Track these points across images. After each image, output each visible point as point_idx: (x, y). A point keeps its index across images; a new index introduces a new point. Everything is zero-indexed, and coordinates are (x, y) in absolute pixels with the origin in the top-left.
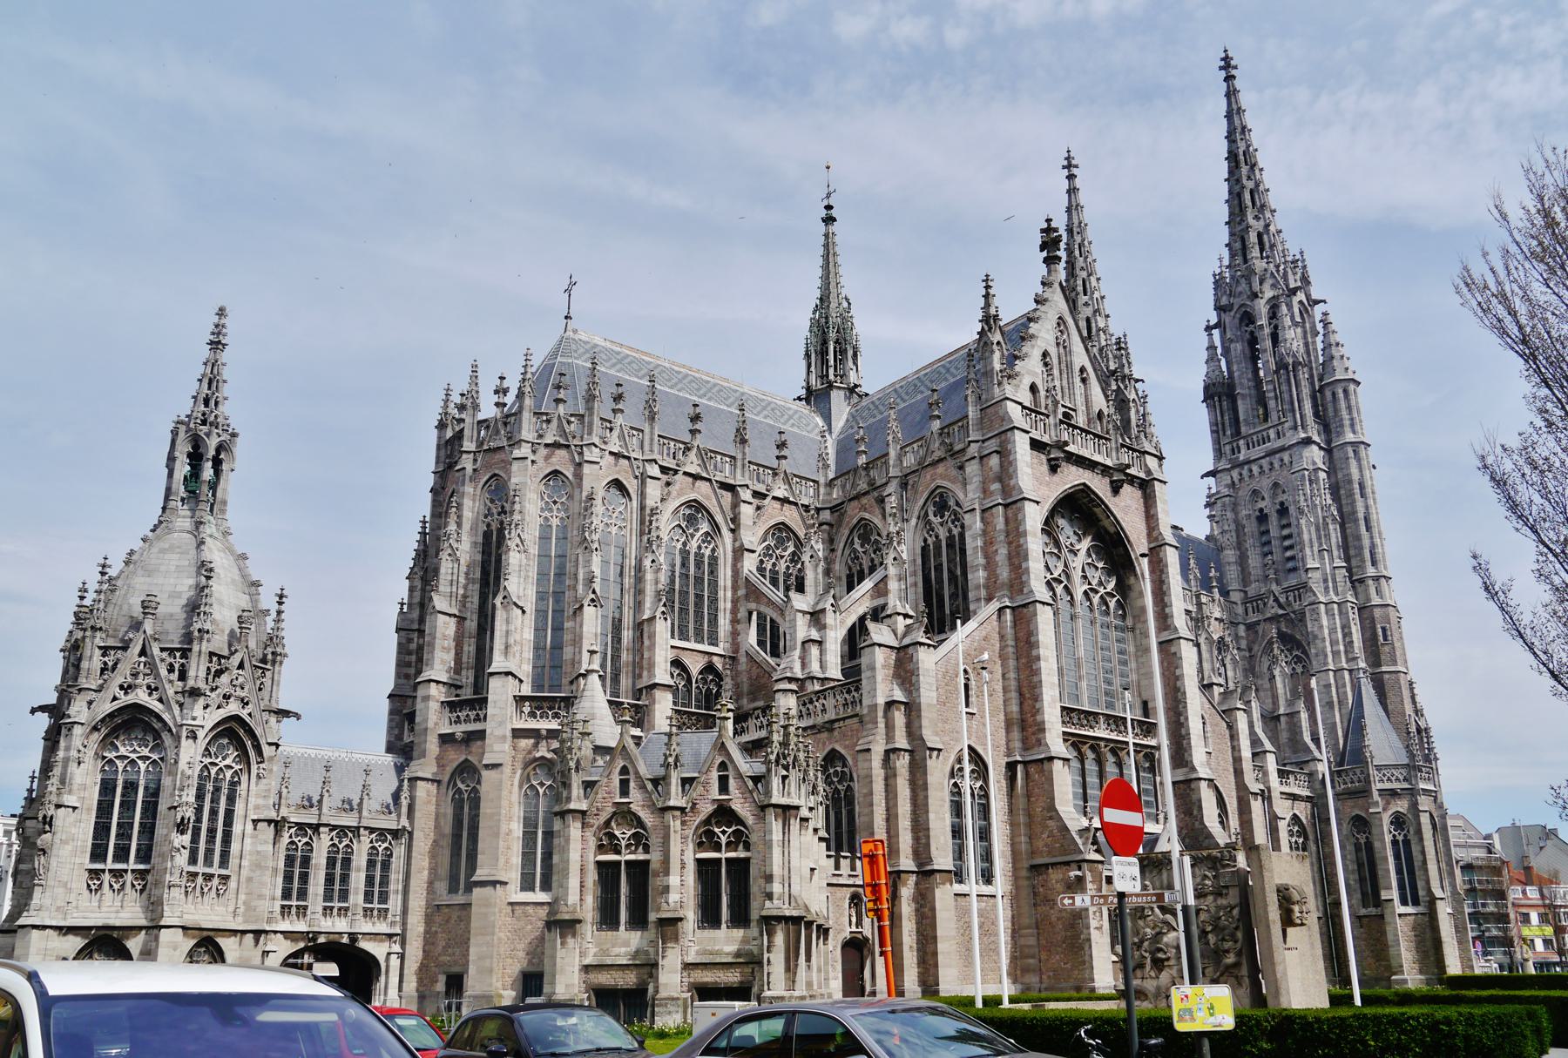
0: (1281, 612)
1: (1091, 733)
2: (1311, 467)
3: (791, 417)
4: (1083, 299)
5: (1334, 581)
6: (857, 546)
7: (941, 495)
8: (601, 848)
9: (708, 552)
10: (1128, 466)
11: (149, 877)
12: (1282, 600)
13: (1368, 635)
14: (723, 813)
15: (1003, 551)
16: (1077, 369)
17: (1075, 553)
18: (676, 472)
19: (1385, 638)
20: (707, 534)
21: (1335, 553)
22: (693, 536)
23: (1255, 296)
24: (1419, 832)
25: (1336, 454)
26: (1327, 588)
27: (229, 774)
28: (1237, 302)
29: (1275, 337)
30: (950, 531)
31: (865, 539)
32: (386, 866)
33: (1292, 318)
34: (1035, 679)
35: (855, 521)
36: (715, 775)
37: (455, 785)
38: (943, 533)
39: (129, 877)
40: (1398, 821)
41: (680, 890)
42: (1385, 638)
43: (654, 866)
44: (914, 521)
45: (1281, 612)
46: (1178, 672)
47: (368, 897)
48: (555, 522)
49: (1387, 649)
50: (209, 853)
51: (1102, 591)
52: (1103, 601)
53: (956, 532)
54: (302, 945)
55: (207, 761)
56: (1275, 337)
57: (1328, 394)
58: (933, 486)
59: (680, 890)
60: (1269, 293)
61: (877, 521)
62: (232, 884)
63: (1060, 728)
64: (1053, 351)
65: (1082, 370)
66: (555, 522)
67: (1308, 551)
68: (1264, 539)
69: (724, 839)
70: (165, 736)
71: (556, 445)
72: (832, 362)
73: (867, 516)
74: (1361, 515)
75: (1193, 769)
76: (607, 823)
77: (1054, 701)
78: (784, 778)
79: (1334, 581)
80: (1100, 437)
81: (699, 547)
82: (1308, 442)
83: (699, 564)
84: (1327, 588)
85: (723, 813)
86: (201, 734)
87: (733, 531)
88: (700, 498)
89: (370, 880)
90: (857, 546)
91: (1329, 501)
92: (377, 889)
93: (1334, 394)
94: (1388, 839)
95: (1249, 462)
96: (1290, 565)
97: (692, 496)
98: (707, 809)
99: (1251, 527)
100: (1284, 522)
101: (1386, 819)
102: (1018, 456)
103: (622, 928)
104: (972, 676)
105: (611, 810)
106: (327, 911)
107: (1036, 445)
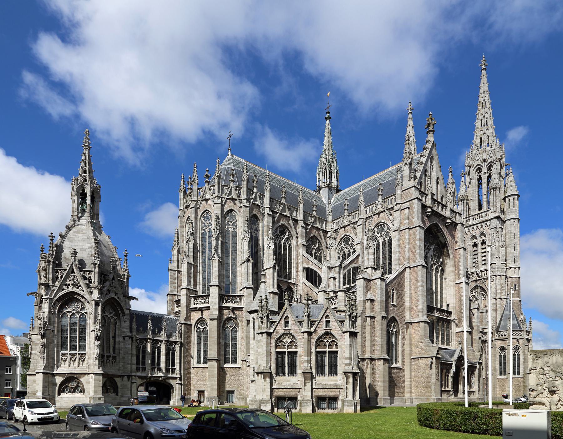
6: (343, 245)
7: (381, 225)
8: (277, 346)
9: (288, 245)
12: (480, 274)
14: (328, 334)
18: (277, 213)
20: (287, 238)
30: (384, 239)
31: (347, 242)
35: (342, 236)
36: (324, 320)
38: (381, 240)
43: (298, 353)
52: (437, 268)
53: (387, 239)
58: (378, 222)
61: (353, 235)
69: (327, 344)
72: (328, 177)
73: (348, 234)
76: (280, 337)
83: (285, 249)
85: (328, 334)
90: (343, 245)
96: (484, 262)
98: (321, 332)
105: (283, 332)
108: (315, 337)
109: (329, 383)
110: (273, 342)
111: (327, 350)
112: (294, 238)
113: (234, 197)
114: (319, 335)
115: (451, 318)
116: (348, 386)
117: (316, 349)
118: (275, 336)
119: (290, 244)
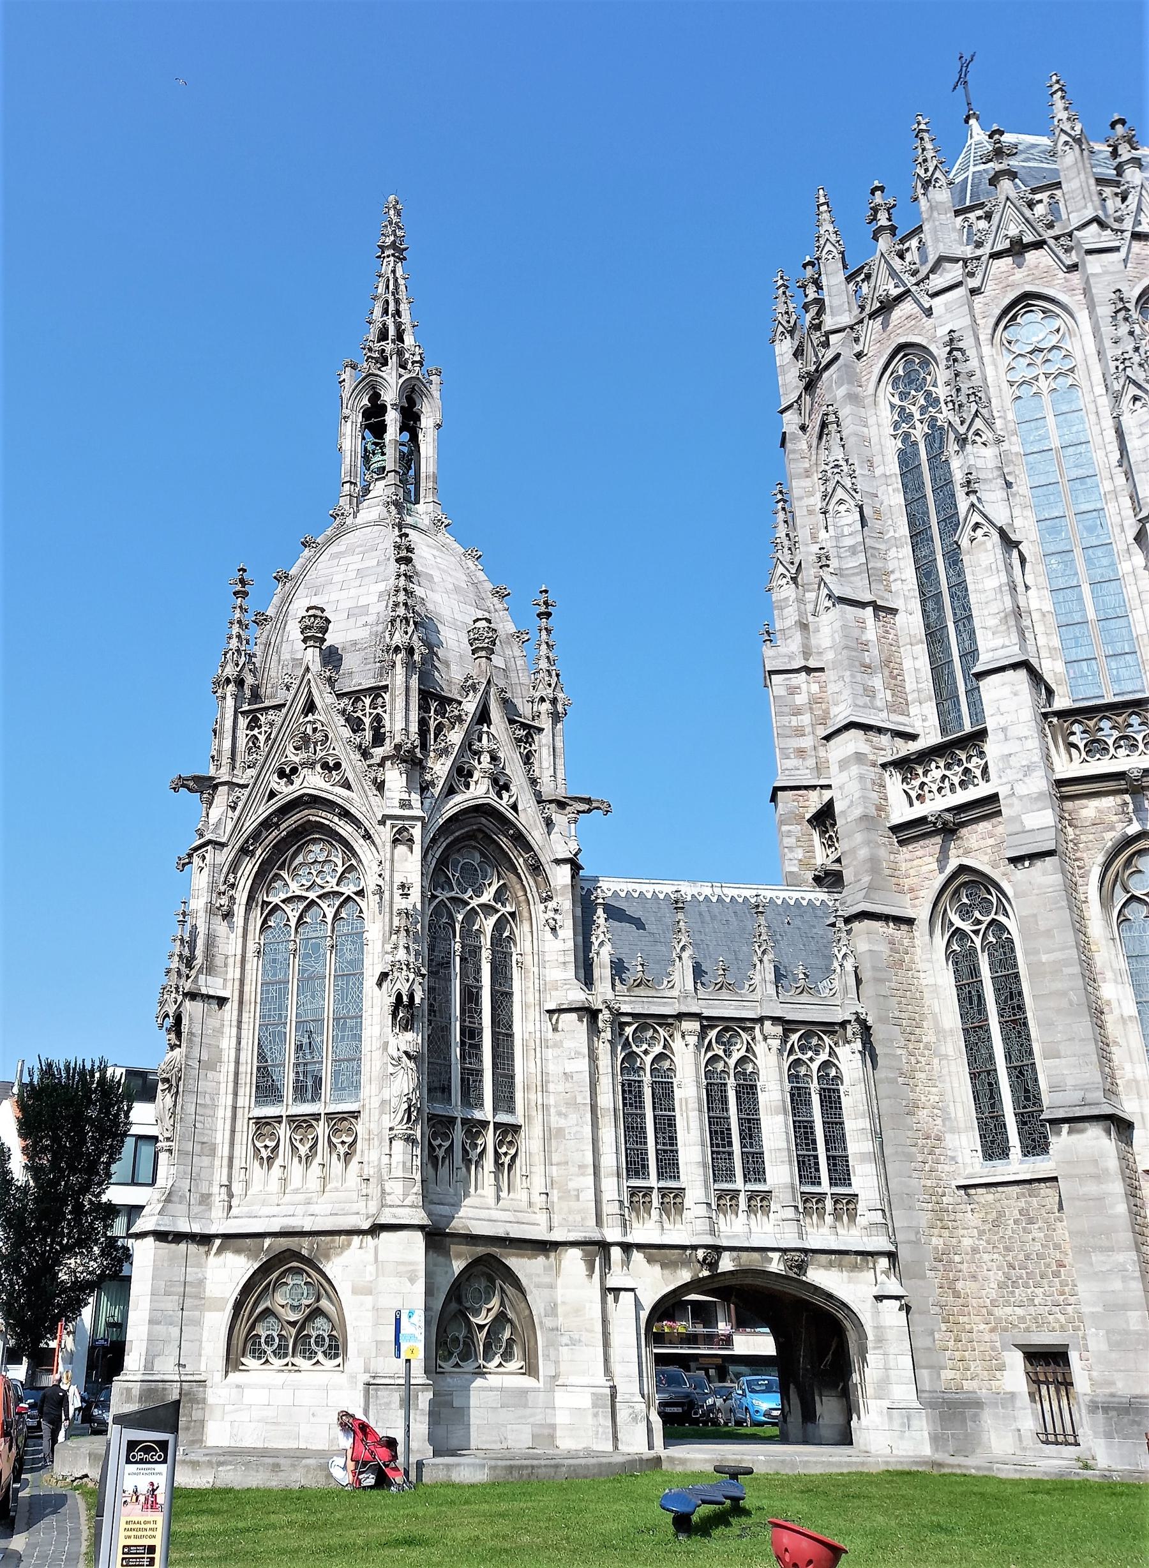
11: (360, 1127)
27: (489, 923)
32: (831, 1101)
37: (947, 923)
39: (322, 1129)
47: (806, 1168)
50: (471, 1078)
54: (685, 1276)
55: (443, 895)
62: (530, 1142)
70: (360, 845)
71: (1017, 249)
86: (417, 832)
89: (803, 1132)
92: (822, 1157)
106: (725, 1201)
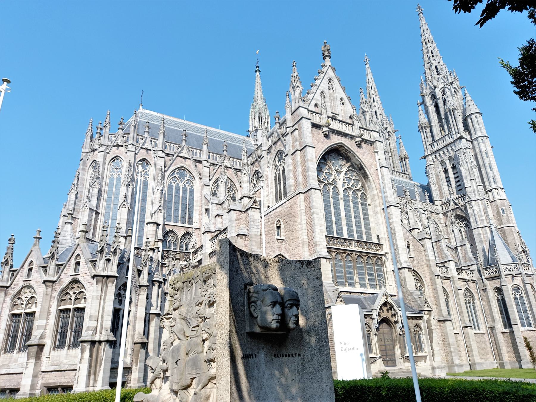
0: (457, 207)
1: (348, 248)
2: (464, 148)
3: (240, 141)
4: (373, 105)
5: (478, 191)
10: (362, 135)
12: (456, 201)
13: (496, 212)
15: (300, 169)
16: (339, 99)
17: (339, 173)
18: (174, 155)
19: (504, 213)
21: (477, 180)
22: (182, 182)
23: (435, 87)
24: (526, 293)
25: (475, 143)
26: (475, 194)
28: (429, 91)
29: (445, 102)
33: (451, 93)
34: (312, 223)
36: (73, 262)
40: (516, 288)
41: (45, 327)
42: (504, 213)
44: (271, 167)
45: (457, 207)
46: (391, 221)
48: (115, 176)
49: (505, 217)
51: (354, 189)
56: (445, 102)
57: (469, 120)
58: (277, 151)
59: (45, 327)
60: (441, 86)
63: (325, 244)
64: (327, 91)
65: (341, 100)
66: (115, 176)
67: (465, 181)
68: (448, 179)
74: (487, 164)
75: (402, 264)
76: (19, 292)
77: (322, 232)
78: (109, 260)
79: (478, 191)
80: (349, 124)
81: (185, 185)
82: (461, 138)
84: (475, 194)
87: (201, 178)
88: (185, 166)
91: (473, 160)
93: (471, 119)
94: (512, 297)
95: (438, 150)
97: (181, 165)
98: (66, 279)
99: (443, 175)
100: (455, 172)
101: (510, 287)
102: (305, 129)
103: (15, 352)
104: (282, 223)
105: (21, 284)
107: (315, 126)
108: (59, 287)
109: (65, 362)
110: (8, 299)
111: (71, 307)
112: (197, 178)
113: (120, 144)
114: (64, 285)
115: (382, 253)
116: (81, 365)
117: (58, 305)
118: (12, 292)
119: (192, 186)
